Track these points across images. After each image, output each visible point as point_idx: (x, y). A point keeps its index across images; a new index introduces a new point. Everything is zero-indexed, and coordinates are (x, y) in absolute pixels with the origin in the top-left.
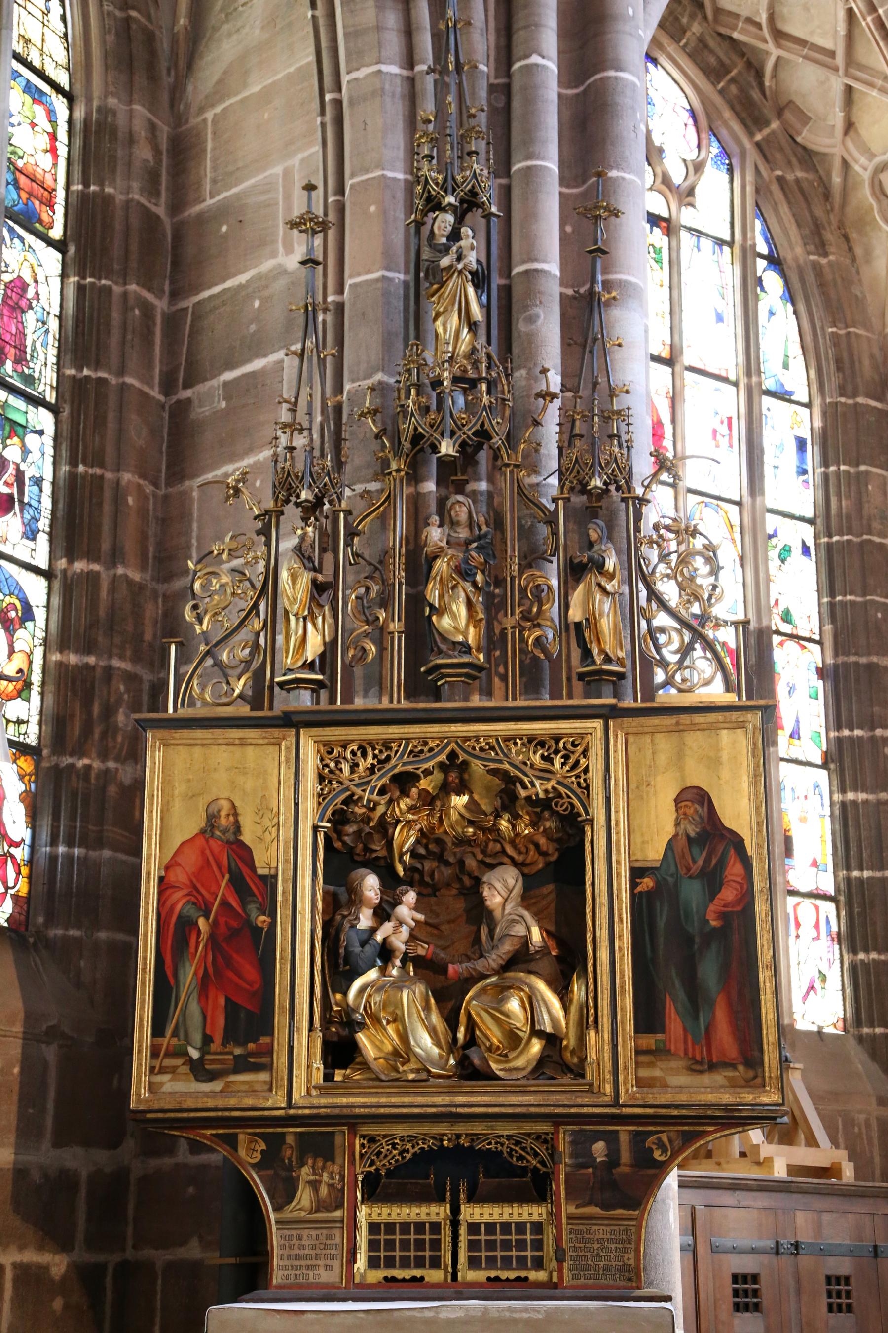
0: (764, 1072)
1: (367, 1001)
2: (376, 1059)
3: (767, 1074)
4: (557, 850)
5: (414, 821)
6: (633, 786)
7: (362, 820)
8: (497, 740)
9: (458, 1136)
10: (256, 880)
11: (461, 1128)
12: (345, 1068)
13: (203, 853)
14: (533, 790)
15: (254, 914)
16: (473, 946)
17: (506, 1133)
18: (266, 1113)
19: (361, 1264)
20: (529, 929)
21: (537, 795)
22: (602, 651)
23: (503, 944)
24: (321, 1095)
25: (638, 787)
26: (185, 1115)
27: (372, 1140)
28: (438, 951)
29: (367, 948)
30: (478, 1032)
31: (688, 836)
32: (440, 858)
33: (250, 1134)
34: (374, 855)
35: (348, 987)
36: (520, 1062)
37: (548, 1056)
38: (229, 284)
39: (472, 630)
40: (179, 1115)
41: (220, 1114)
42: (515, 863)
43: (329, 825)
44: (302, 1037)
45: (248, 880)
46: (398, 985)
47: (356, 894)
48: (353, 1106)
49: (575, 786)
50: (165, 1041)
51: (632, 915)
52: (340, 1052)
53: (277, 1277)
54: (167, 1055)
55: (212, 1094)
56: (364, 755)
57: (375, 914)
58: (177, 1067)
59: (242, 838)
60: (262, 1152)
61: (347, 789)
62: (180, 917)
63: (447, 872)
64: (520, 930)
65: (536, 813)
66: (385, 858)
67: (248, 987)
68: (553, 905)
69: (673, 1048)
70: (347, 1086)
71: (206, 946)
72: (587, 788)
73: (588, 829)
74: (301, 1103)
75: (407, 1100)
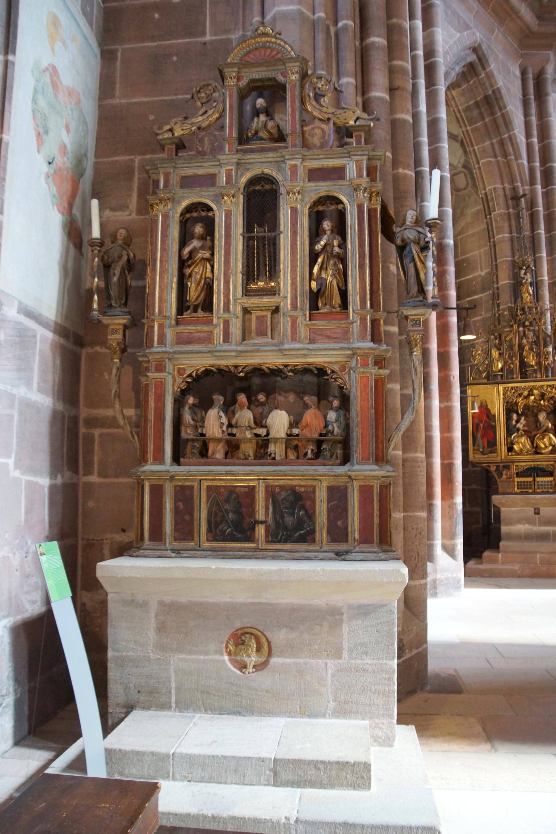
11: (536, 463)
19: (516, 489)
32: (529, 410)
38: (467, 278)
44: (503, 447)
46: (522, 436)
52: (510, 449)
53: (500, 491)
70: (511, 455)
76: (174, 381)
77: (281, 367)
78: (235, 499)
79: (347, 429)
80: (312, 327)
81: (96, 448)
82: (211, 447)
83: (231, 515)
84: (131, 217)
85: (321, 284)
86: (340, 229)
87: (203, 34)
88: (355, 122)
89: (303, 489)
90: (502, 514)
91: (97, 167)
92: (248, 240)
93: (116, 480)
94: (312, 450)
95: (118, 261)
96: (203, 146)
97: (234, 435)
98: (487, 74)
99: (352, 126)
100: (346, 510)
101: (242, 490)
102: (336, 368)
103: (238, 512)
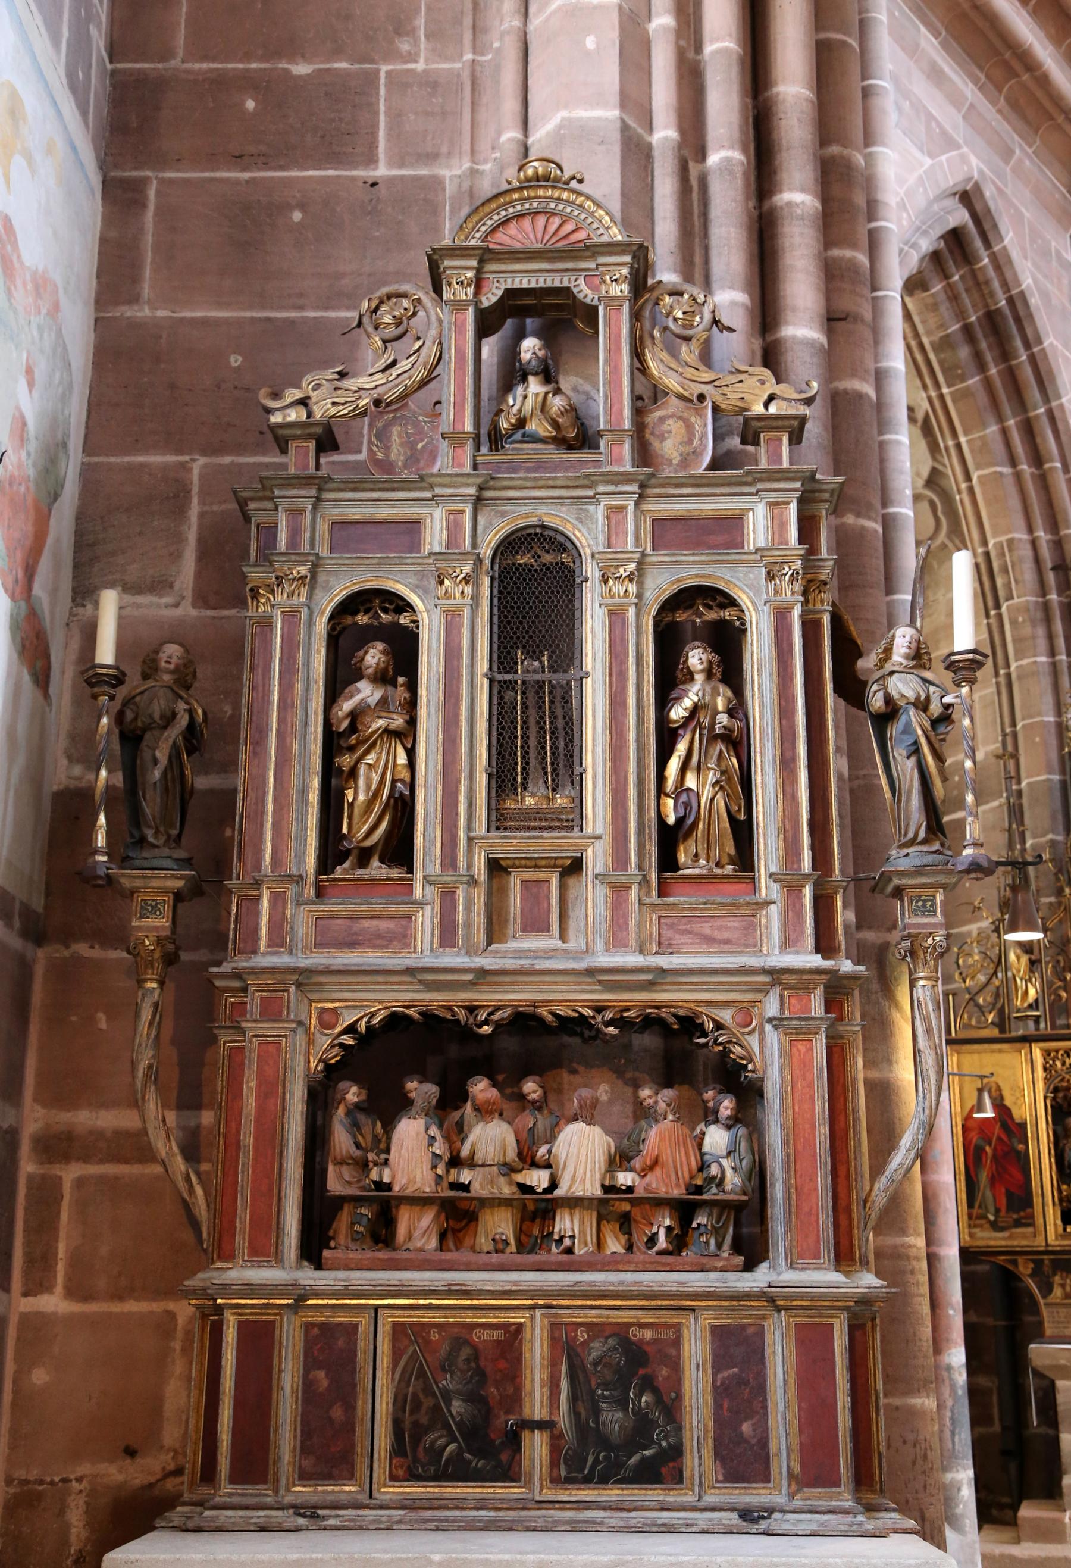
44: (1050, 1209)
50: (975, 1211)
53: (1048, 1332)
54: (978, 1218)
55: (1004, 1239)
76: (310, 1042)
77: (588, 1012)
78: (468, 1360)
79: (758, 1175)
80: (664, 913)
81: (64, 1216)
82: (405, 1219)
83: (457, 1406)
84: (178, 612)
85: (687, 805)
86: (729, 670)
87: (371, 160)
88: (766, 405)
89: (648, 1334)
90: (1060, 1398)
91: (88, 476)
92: (500, 689)
93: (116, 1308)
94: (669, 1229)
95: (165, 727)
96: (387, 449)
97: (466, 1188)
98: (994, 257)
99: (760, 418)
100: (761, 1389)
101: (489, 1336)
102: (726, 1016)
103: (474, 1398)
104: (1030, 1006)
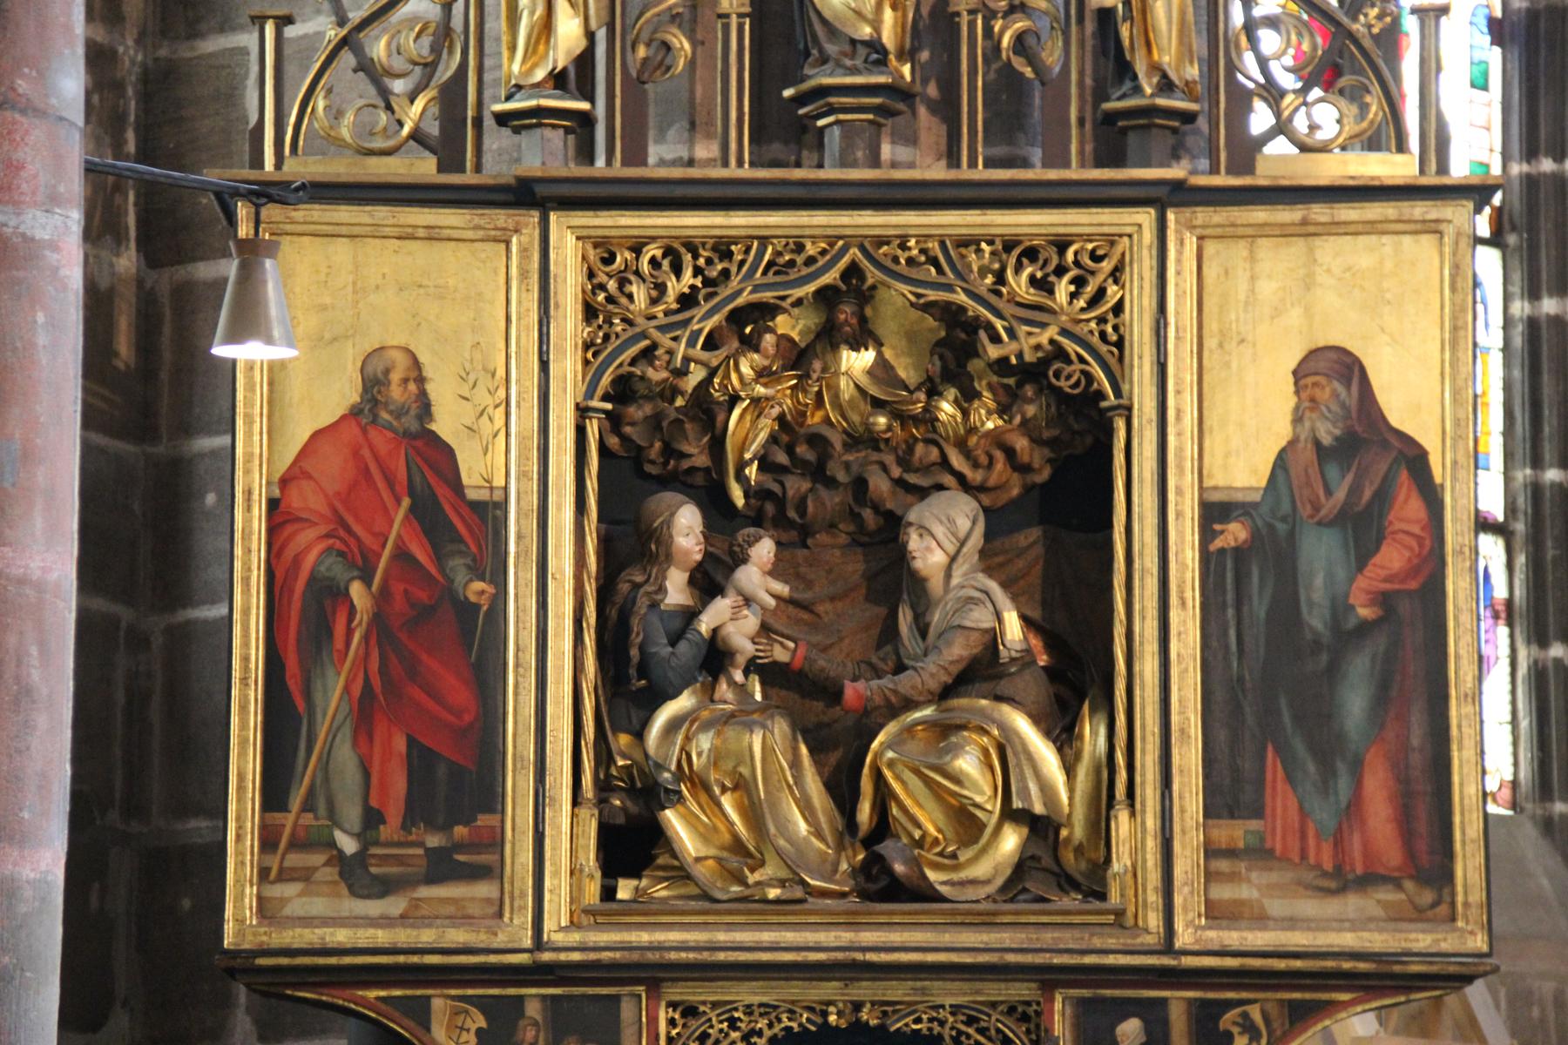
0: (1453, 894)
1: (682, 749)
2: (698, 860)
3: (1460, 899)
4: (1049, 461)
5: (767, 399)
6: (1210, 343)
7: (661, 395)
8: (943, 244)
9: (858, 1006)
10: (465, 511)
11: (864, 990)
12: (639, 877)
13: (356, 453)
14: (1014, 346)
15: (460, 577)
16: (879, 647)
17: (948, 1001)
18: (493, 959)
20: (999, 617)
21: (1020, 355)
22: (1156, 68)
23: (949, 644)
24: (598, 926)
25: (1221, 345)
26: (333, 961)
27: (690, 1011)
28: (814, 654)
29: (683, 646)
30: (895, 811)
31: (1317, 443)
32: (818, 473)
33: (453, 998)
34: (686, 464)
35: (646, 723)
36: (981, 870)
37: (1032, 857)
39: (888, 15)
40: (321, 961)
41: (401, 959)
42: (964, 484)
43: (609, 406)
44: (561, 815)
45: (447, 507)
46: (742, 717)
47: (658, 543)
48: (660, 948)
49: (1095, 340)
50: (288, 820)
51: (1203, 594)
52: (630, 844)
54: (296, 845)
56: (677, 270)
57: (692, 582)
58: (316, 869)
59: (433, 427)
60: (479, 1032)
61: (644, 335)
62: (313, 579)
63: (832, 500)
64: (981, 618)
65: (1007, 387)
66: (707, 470)
67: (451, 718)
68: (1039, 568)
69: (1278, 847)
70: (641, 907)
71: (366, 638)
72: (1120, 344)
73: (1120, 424)
74: (559, 938)
75: (767, 937)
104: (558, 80)
